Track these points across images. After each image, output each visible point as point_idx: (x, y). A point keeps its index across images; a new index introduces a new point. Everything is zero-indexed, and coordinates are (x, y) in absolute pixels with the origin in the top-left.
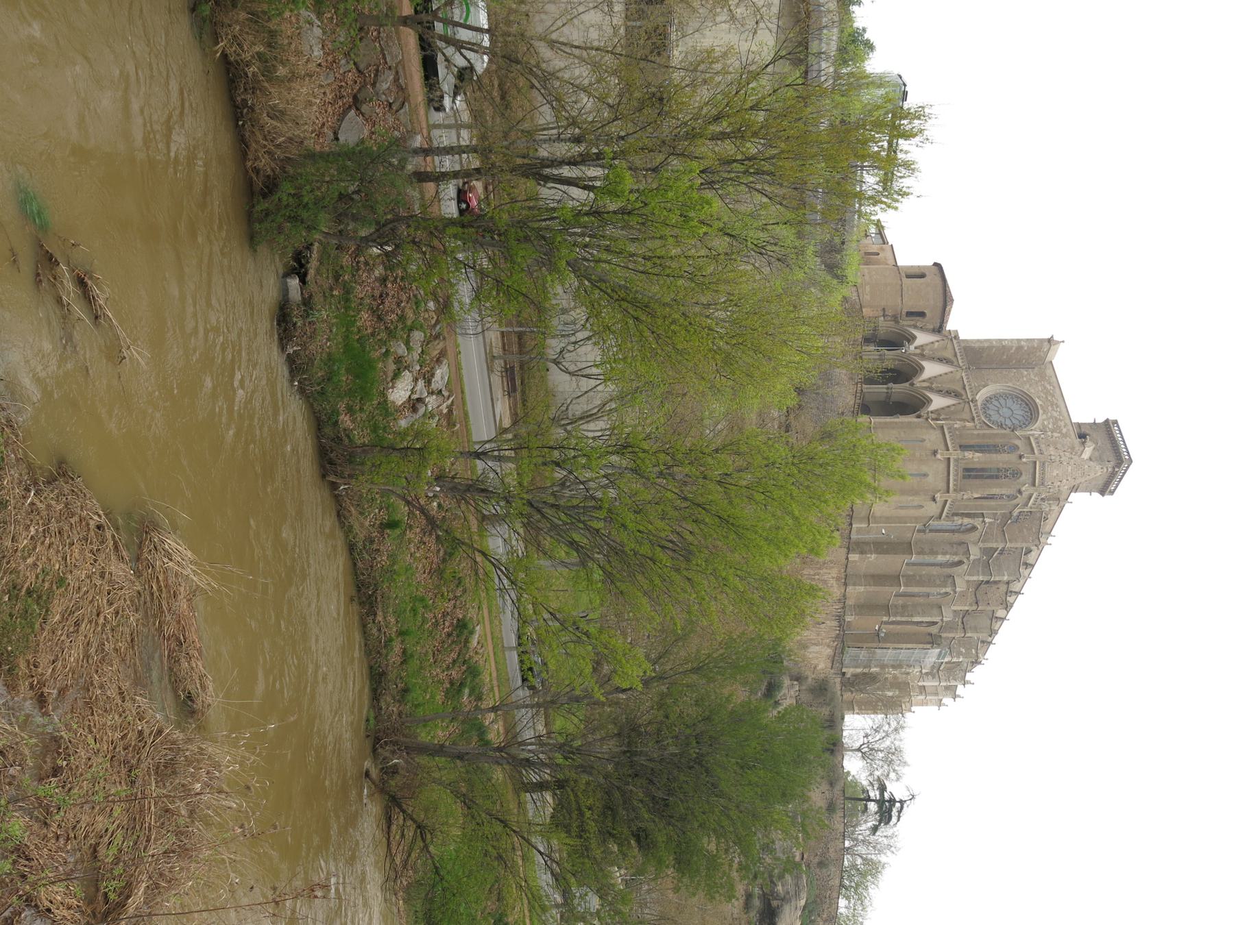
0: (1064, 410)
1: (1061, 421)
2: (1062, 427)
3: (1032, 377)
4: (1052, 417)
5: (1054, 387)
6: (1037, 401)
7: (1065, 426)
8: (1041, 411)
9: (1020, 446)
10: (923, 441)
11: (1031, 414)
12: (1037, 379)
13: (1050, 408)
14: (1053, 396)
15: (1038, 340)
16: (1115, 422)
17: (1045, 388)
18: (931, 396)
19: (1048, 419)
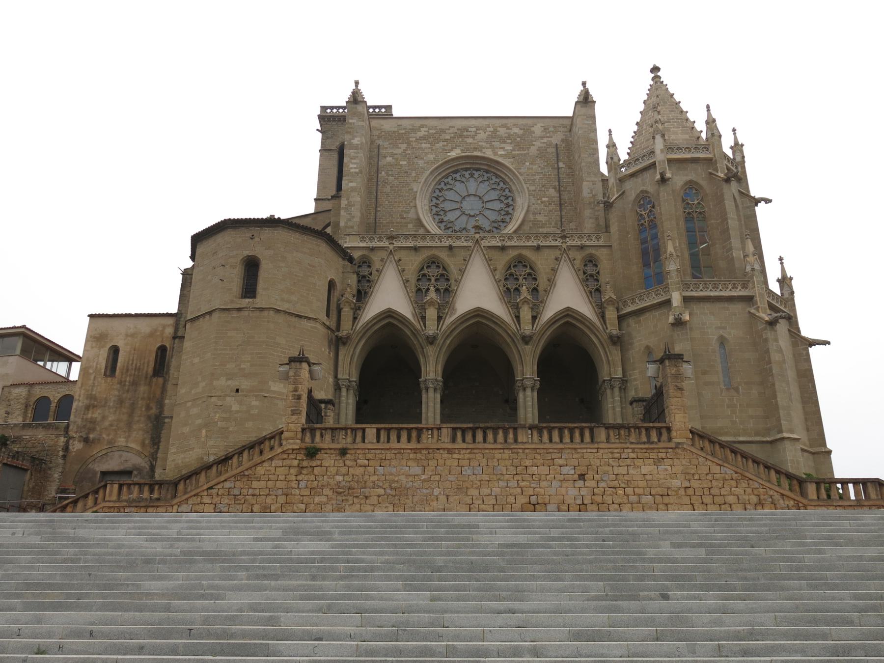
0: (473, 122)
1: (495, 131)
2: (512, 132)
3: (398, 151)
5: (423, 126)
6: (454, 154)
7: (508, 128)
9: (689, 178)
10: (722, 341)
11: (478, 170)
12: (404, 146)
13: (470, 140)
14: (443, 131)
16: (324, 108)
17: (423, 138)
19: (493, 148)
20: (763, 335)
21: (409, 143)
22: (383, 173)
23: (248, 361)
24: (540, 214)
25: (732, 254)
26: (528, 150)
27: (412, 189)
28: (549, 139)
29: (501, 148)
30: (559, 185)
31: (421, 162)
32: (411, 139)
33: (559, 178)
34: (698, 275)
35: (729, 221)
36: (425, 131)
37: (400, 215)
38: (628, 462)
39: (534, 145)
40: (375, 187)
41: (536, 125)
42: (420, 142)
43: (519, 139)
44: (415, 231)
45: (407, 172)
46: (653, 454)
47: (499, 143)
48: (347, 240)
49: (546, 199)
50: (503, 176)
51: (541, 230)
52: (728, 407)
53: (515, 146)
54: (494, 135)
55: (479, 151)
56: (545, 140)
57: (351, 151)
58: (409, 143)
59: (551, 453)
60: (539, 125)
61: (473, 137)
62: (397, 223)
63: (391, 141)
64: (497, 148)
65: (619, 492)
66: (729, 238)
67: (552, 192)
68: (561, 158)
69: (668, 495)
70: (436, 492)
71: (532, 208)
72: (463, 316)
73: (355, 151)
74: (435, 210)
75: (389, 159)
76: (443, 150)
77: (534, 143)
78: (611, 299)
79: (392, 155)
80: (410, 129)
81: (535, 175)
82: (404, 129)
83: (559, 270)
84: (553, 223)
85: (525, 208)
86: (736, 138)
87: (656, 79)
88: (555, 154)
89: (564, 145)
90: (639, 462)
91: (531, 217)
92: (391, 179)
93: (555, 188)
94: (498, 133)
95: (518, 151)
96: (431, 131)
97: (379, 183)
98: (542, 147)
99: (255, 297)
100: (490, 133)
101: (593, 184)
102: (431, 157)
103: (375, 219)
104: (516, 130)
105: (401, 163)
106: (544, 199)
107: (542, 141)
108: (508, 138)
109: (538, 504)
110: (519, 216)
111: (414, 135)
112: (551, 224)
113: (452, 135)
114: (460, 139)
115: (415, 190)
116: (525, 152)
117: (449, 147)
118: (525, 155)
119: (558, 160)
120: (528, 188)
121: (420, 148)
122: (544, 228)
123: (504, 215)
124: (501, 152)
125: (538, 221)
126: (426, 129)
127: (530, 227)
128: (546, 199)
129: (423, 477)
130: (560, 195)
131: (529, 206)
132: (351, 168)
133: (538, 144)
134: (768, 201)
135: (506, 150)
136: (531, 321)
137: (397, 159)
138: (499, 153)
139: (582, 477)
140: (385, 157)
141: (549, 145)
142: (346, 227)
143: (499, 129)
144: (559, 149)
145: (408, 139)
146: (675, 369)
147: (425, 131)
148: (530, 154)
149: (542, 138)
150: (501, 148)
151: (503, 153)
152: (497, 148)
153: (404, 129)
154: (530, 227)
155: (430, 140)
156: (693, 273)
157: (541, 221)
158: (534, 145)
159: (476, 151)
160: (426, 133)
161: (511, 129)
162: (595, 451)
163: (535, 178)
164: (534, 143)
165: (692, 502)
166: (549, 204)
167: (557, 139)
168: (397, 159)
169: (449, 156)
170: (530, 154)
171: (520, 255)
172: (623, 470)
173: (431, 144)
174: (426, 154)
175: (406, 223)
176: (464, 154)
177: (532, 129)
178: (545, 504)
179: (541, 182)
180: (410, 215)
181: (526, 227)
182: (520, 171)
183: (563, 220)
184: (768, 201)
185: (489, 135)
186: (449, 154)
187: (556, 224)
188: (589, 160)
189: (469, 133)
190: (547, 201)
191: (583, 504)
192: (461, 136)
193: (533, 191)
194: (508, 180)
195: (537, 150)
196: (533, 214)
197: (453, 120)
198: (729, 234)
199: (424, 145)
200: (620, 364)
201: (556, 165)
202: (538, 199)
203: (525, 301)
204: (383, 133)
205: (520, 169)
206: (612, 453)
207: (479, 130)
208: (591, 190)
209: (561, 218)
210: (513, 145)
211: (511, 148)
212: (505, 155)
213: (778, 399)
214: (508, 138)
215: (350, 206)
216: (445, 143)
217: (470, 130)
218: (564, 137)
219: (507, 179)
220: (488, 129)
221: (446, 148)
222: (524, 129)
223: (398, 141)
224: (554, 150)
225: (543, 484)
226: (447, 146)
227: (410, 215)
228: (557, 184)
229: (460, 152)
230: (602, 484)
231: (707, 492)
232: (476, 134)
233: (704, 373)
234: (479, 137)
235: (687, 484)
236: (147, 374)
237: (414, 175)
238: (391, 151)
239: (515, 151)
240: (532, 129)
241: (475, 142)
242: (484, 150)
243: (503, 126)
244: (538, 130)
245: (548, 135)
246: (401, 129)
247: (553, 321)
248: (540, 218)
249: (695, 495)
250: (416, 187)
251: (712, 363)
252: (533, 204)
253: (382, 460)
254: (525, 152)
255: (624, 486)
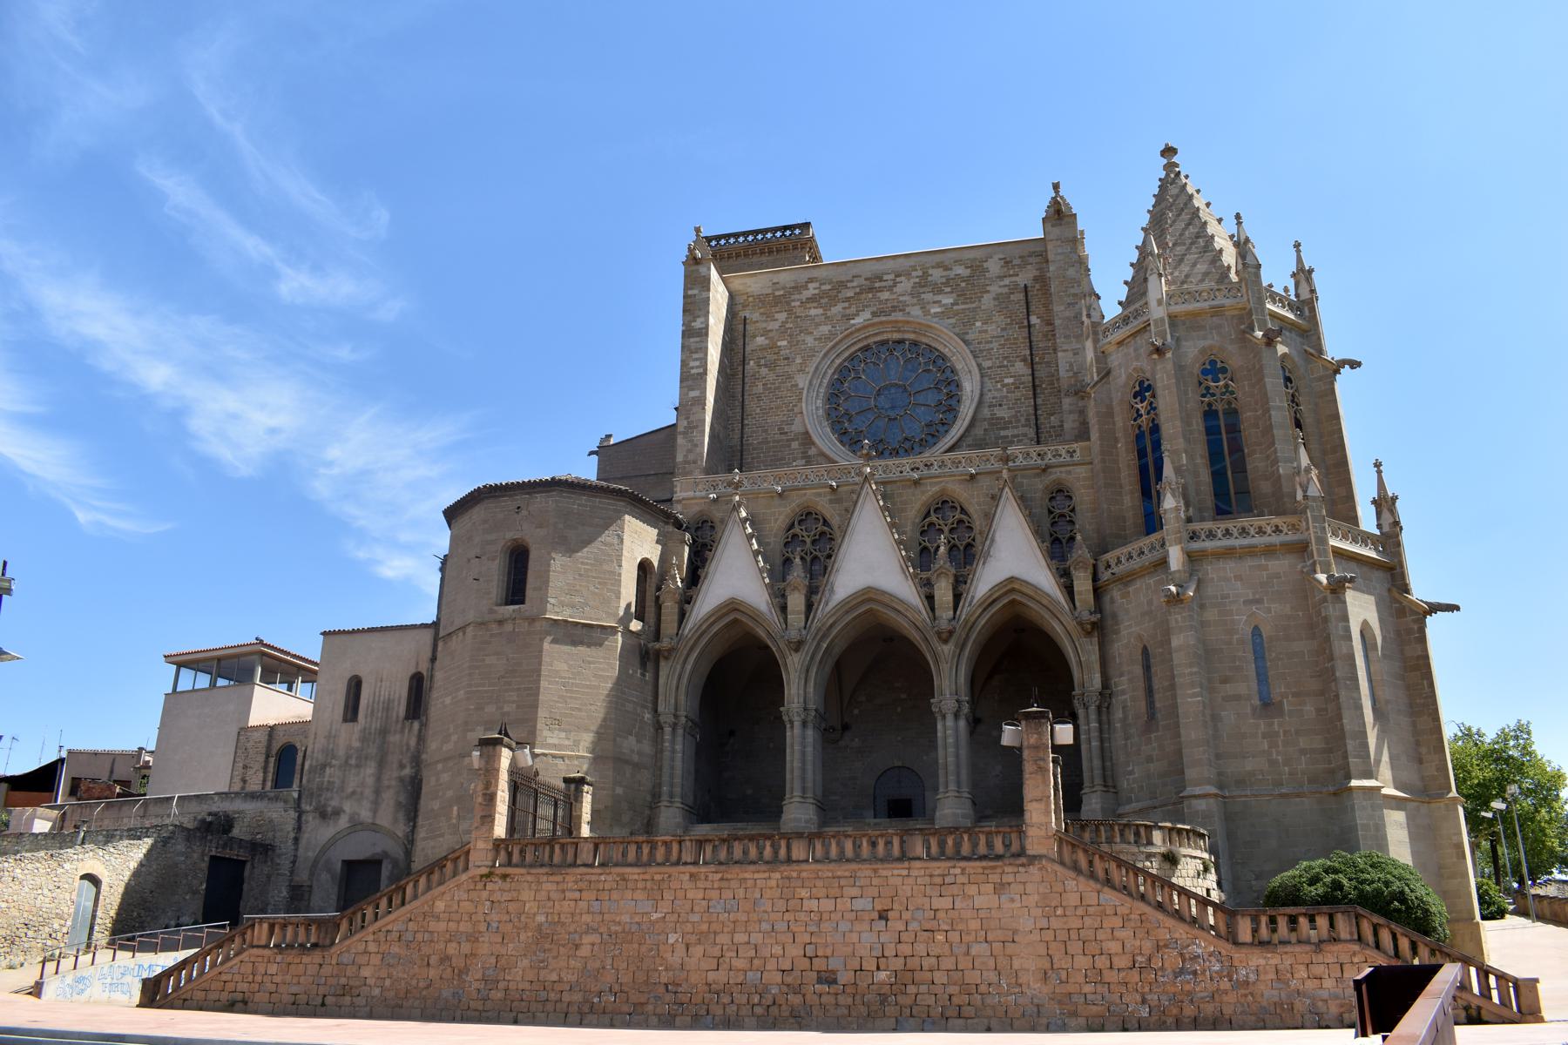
0: (890, 265)
1: (925, 274)
2: (952, 274)
4: (915, 293)
5: (811, 280)
6: (858, 320)
7: (947, 269)
8: (898, 316)
12: (782, 316)
13: (885, 295)
15: (685, 289)
17: (809, 300)
18: (986, 580)
19: (924, 307)
20: (1323, 610)
21: (790, 311)
22: (752, 362)
23: (513, 702)
24: (1000, 405)
25: (1278, 470)
26: (980, 301)
27: (797, 385)
28: (1014, 279)
29: (934, 302)
30: (1031, 354)
31: (810, 340)
32: (793, 304)
33: (1030, 342)
34: (1223, 507)
35: (1273, 413)
36: (815, 289)
37: (779, 429)
38: (955, 889)
39: (988, 292)
40: (740, 387)
41: (991, 257)
42: (808, 306)
43: (963, 284)
44: (802, 453)
45: (788, 359)
46: (995, 876)
47: (931, 294)
48: (678, 489)
49: (1010, 380)
50: (940, 348)
51: (1003, 433)
52: (1264, 738)
53: (958, 296)
54: (924, 283)
55: (900, 310)
56: (1007, 281)
57: (692, 340)
58: (790, 311)
59: (839, 877)
60: (996, 257)
61: (890, 289)
62: (774, 441)
63: (762, 310)
64: (928, 303)
65: (939, 937)
66: (1273, 443)
67: (1021, 368)
68: (1032, 308)
69: (1013, 941)
70: (672, 939)
71: (988, 397)
72: (844, 602)
73: (698, 339)
74: (834, 414)
75: (760, 340)
76: (843, 316)
77: (988, 288)
78: (1081, 559)
79: (765, 333)
80: (793, 288)
81: (991, 342)
82: (783, 288)
83: (997, 516)
84: (1023, 420)
85: (976, 400)
86: (1299, 260)
87: (1170, 167)
88: (1023, 303)
89: (1037, 286)
90: (972, 890)
91: (986, 412)
92: (764, 371)
93: (1024, 360)
94: (930, 278)
95: (967, 303)
96: (824, 287)
97: (746, 380)
98: (1001, 294)
99: (523, 602)
100: (917, 280)
101: (1075, 354)
102: (825, 329)
103: (742, 437)
104: (960, 270)
105: (779, 344)
106: (1007, 381)
107: (1002, 283)
108: (946, 284)
109: (817, 956)
110: (966, 411)
111: (797, 297)
112: (1019, 421)
113: (858, 290)
114: (870, 295)
115: (801, 386)
116: (974, 305)
117: (853, 310)
118: (974, 310)
119: (1028, 312)
120: (979, 365)
121: (807, 316)
122: (1008, 428)
123: (945, 412)
124: (935, 309)
125: (997, 419)
126: (816, 285)
127: (985, 430)
128: (1010, 380)
129: (655, 916)
130: (1033, 370)
131: (982, 395)
132: (692, 368)
133: (995, 289)
134: (1354, 364)
135: (947, 304)
136: (951, 605)
137: (771, 339)
138: (933, 311)
139: (883, 916)
140: (755, 337)
141: (1013, 288)
142: (686, 462)
143: (930, 272)
144: (1030, 294)
145: (788, 303)
146: (1035, 736)
147: (815, 289)
148: (983, 307)
149: (1001, 278)
150: (934, 302)
151: (939, 310)
152: (928, 303)
153: (783, 288)
154: (985, 430)
155: (823, 301)
156: (1216, 505)
157: (1003, 418)
158: (988, 292)
159: (895, 311)
160: (817, 291)
161: (951, 269)
162: (905, 872)
163: (988, 346)
164: (988, 288)
165: (1050, 952)
166: (1016, 388)
167: (1025, 277)
168: (771, 339)
169: (854, 325)
170: (983, 307)
171: (943, 491)
172: (945, 903)
173: (826, 308)
174: (818, 325)
175: (788, 440)
176: (876, 320)
177: (985, 265)
178: (827, 957)
179: (1001, 351)
180: (793, 428)
181: (978, 431)
182: (967, 337)
183: (1039, 412)
184: (1354, 364)
185: (915, 283)
186: (852, 322)
187: (1027, 420)
188: (1067, 314)
189: (883, 284)
190: (1012, 384)
191: (883, 956)
192: (871, 289)
193: (989, 368)
194: (949, 355)
195: (994, 299)
196: (989, 407)
197: (858, 265)
198: (1273, 436)
199: (813, 312)
200: (1097, 667)
201: (1026, 323)
202: (997, 382)
203: (942, 573)
204: (751, 299)
205: (967, 333)
206: (931, 876)
207: (898, 276)
208: (1071, 365)
209: (1036, 410)
210: (954, 295)
211: (951, 301)
212: (943, 312)
213: (1344, 721)
214: (946, 284)
215: (690, 428)
216: (846, 305)
217: (885, 277)
218: (1037, 273)
219: (945, 351)
220: (914, 274)
221: (848, 312)
222: (972, 266)
223: (773, 310)
224: (1022, 296)
225: (826, 926)
226: (850, 308)
227: (793, 428)
228: (1028, 352)
229: (869, 316)
230: (914, 926)
231: (1074, 935)
232: (895, 285)
233: (1225, 681)
234: (899, 289)
235: (1044, 923)
236: (398, 717)
237: (798, 361)
238: (764, 325)
239: (957, 304)
240: (985, 265)
241: (895, 296)
242: (907, 310)
243: (938, 265)
244: (994, 267)
245: (1011, 273)
246: (778, 290)
247: (989, 602)
248: (1003, 413)
249: (1055, 941)
250: (802, 381)
251: (1237, 663)
252: (990, 391)
253: (598, 890)
254: (974, 305)
255: (946, 928)
